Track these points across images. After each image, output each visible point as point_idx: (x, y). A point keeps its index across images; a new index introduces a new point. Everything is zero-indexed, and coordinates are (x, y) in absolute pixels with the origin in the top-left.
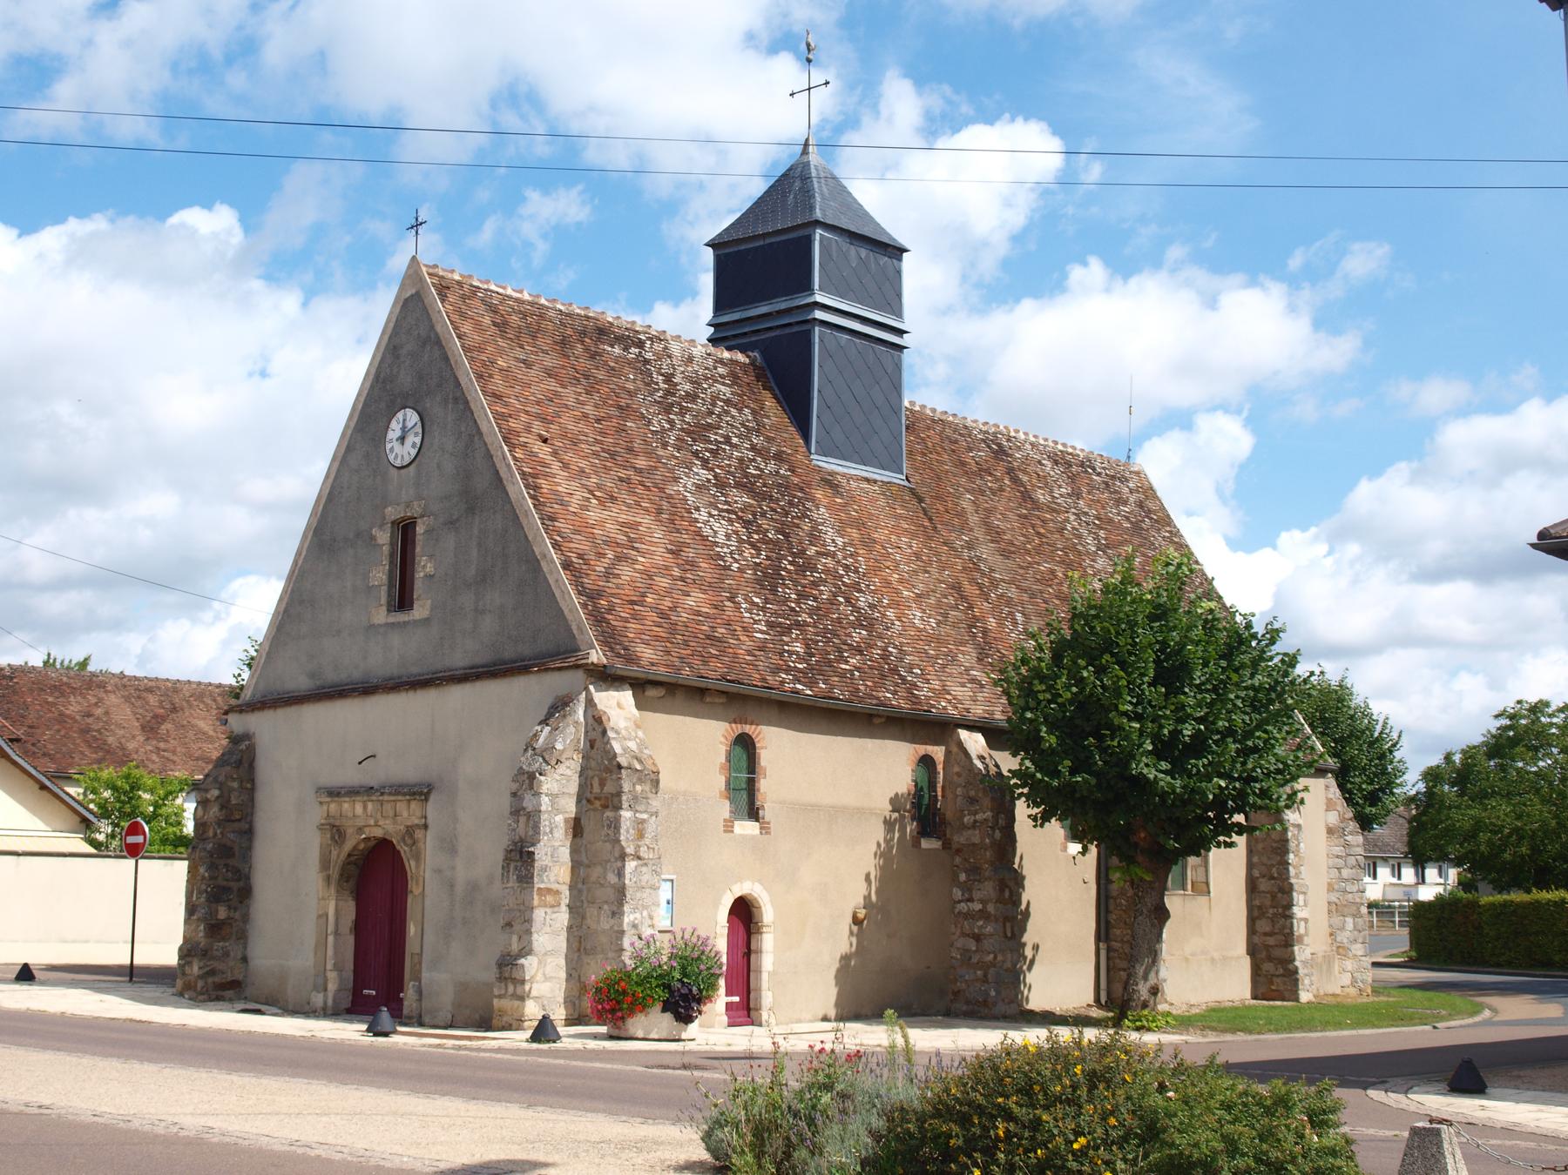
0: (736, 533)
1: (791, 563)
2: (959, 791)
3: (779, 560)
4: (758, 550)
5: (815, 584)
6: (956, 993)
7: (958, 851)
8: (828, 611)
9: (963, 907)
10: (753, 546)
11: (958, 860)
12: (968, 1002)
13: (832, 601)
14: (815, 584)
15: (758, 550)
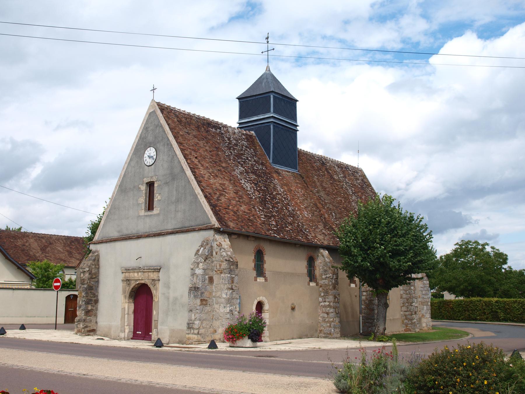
0: (253, 187)
1: (269, 197)
2: (321, 268)
3: (266, 195)
4: (260, 193)
5: (277, 203)
6: (321, 331)
7: (321, 286)
8: (281, 212)
9: (322, 304)
10: (258, 191)
11: (321, 289)
12: (324, 334)
13: (282, 208)
14: (277, 203)
15: (260, 193)
